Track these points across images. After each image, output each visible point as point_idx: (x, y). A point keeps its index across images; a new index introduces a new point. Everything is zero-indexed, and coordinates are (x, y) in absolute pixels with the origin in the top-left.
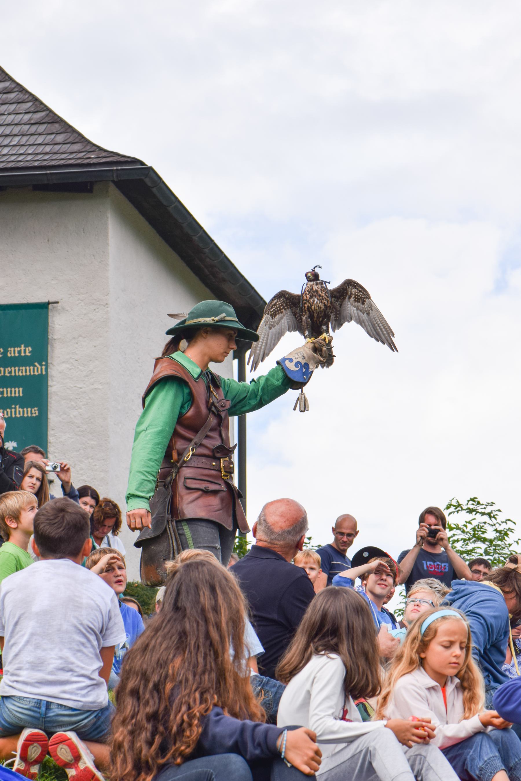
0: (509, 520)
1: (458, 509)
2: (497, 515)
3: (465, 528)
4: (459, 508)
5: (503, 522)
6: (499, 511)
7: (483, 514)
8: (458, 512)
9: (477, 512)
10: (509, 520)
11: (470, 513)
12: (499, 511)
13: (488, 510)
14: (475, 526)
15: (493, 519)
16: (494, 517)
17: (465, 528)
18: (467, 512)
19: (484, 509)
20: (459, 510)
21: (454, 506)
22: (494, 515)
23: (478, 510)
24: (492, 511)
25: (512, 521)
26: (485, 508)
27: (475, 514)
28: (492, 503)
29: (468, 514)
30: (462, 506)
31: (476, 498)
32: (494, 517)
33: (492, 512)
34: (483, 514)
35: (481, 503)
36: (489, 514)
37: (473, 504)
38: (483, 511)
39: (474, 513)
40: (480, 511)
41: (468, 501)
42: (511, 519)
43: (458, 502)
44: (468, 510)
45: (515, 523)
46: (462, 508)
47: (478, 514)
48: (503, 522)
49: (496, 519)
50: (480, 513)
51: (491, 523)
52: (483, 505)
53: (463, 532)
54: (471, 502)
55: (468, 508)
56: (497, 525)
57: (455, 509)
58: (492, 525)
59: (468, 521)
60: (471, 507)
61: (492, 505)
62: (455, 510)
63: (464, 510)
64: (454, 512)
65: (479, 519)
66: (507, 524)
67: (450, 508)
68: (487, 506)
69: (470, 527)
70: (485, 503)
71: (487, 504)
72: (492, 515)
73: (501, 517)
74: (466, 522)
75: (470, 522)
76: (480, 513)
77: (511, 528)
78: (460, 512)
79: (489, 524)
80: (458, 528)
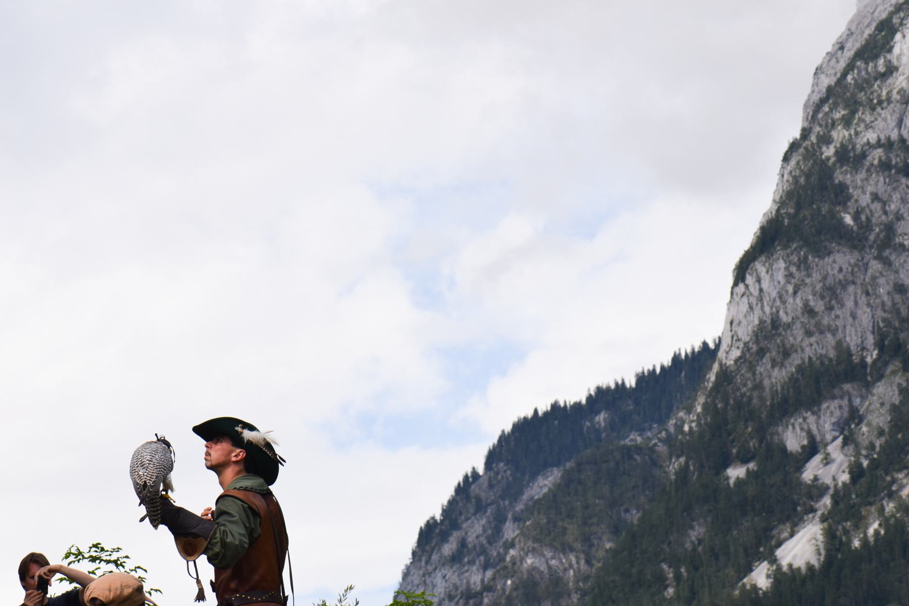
0: (139, 567)
1: (79, 557)
2: (124, 562)
4: (80, 557)
5: (132, 570)
6: (127, 557)
7: (108, 562)
8: (79, 562)
9: (101, 560)
10: (139, 567)
11: (93, 562)
12: (127, 557)
13: (114, 557)
15: (120, 567)
16: (121, 565)
18: (89, 561)
19: (109, 557)
20: (80, 559)
21: (74, 554)
22: (121, 563)
23: (102, 558)
24: (118, 558)
25: (142, 569)
26: (110, 555)
27: (99, 563)
28: (118, 548)
29: (91, 562)
30: (83, 553)
31: (100, 544)
32: (121, 565)
33: (118, 559)
34: (108, 562)
35: (106, 550)
36: (115, 562)
37: (96, 551)
38: (108, 558)
39: (98, 561)
40: (104, 558)
41: (91, 548)
42: (142, 567)
43: (78, 549)
44: (91, 558)
45: (146, 571)
46: (83, 556)
47: (103, 562)
48: (132, 570)
49: (123, 567)
50: (105, 561)
52: (107, 551)
54: (94, 549)
55: (91, 556)
57: (75, 558)
59: (91, 571)
60: (94, 554)
61: (118, 551)
62: (75, 560)
63: (86, 558)
64: (74, 562)
66: (136, 572)
67: (70, 557)
68: (112, 552)
70: (110, 550)
71: (113, 550)
72: (119, 562)
73: (129, 565)
76: (105, 561)
77: (142, 576)
78: (81, 561)
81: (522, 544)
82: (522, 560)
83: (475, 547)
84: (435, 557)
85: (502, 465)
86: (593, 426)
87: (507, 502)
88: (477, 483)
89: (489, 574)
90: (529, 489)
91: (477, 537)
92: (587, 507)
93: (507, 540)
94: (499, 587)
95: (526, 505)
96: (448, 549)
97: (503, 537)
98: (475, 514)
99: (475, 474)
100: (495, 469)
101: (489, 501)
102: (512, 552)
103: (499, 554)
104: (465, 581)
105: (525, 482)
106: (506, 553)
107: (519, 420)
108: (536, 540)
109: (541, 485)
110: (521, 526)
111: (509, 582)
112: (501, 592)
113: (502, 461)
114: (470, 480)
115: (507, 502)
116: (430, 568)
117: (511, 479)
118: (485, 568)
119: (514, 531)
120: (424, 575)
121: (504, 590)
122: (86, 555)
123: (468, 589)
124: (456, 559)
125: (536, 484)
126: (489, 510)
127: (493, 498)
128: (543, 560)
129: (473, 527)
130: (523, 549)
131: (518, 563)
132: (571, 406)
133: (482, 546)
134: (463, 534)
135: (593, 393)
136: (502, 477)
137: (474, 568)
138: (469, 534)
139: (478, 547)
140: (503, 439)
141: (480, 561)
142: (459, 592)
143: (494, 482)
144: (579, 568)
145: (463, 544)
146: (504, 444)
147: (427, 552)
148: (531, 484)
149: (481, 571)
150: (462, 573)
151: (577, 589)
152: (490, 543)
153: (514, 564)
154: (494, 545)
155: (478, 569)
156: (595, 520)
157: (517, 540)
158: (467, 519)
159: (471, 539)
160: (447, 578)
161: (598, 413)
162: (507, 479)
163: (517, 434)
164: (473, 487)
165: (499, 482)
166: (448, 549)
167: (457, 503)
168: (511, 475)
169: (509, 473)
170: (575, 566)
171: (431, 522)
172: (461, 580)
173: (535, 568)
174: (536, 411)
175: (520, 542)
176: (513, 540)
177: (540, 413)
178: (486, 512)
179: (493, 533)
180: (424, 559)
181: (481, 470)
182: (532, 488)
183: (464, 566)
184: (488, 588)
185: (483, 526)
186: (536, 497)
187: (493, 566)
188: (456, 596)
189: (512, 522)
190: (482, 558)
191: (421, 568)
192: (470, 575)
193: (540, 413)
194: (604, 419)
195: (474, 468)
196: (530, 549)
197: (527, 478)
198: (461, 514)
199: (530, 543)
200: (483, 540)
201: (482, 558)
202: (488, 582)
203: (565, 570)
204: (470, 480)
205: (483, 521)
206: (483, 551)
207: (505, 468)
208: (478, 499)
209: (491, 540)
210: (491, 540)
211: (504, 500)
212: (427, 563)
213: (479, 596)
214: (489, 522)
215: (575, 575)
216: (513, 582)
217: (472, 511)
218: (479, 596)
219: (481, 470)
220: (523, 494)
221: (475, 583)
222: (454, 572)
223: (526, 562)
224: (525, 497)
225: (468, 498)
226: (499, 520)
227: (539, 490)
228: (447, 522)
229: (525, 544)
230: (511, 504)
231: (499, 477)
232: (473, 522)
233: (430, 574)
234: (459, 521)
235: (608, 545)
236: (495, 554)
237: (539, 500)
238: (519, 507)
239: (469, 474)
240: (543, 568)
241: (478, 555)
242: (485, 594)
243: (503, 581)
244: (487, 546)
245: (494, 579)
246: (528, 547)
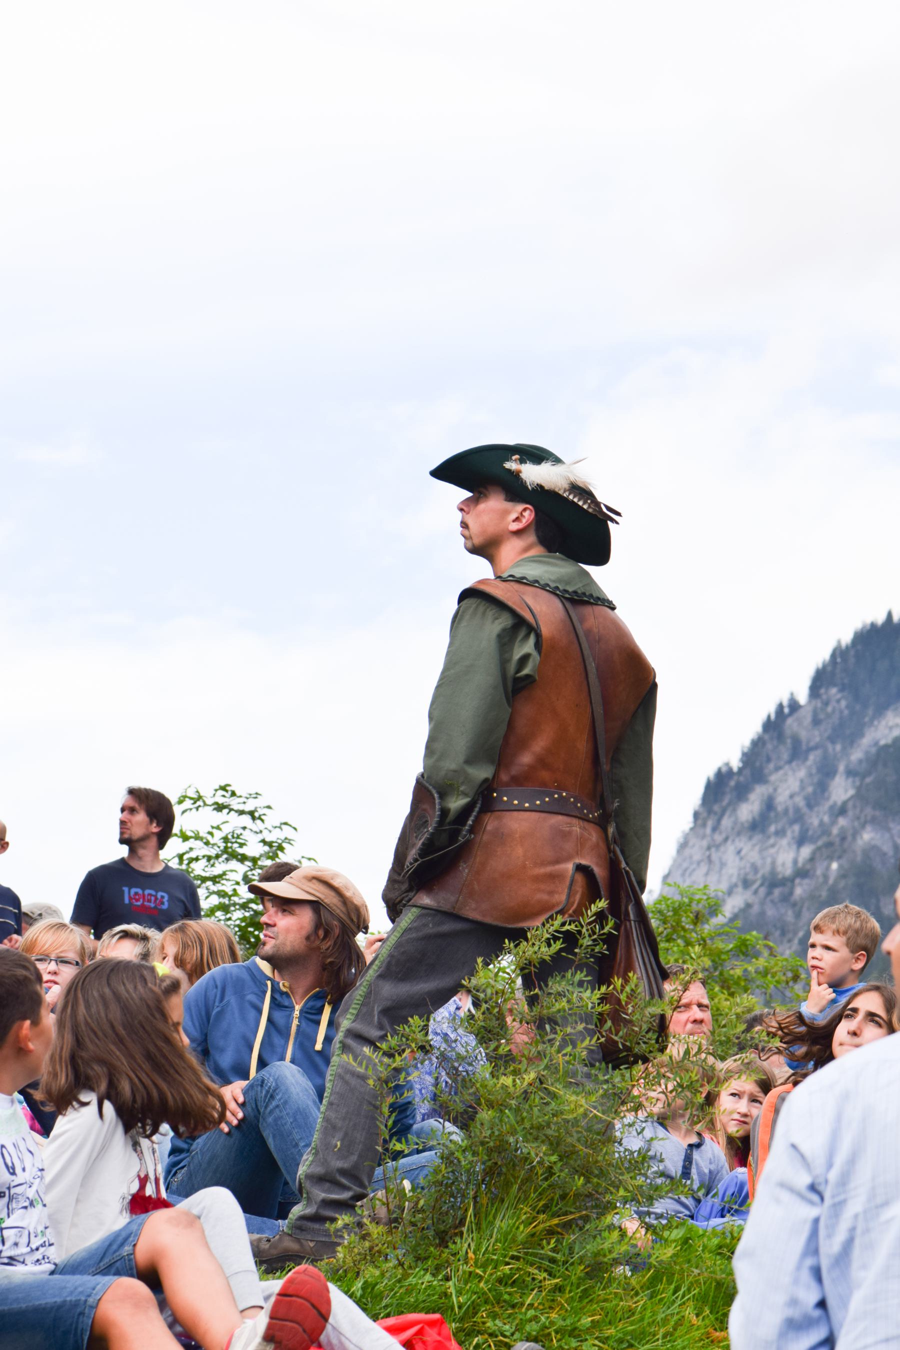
0: (286, 824)
1: (198, 803)
2: (264, 815)
3: (209, 838)
4: (200, 803)
5: (276, 827)
6: (269, 807)
7: (241, 813)
8: (197, 808)
9: (231, 810)
10: (286, 824)
11: (218, 811)
12: (269, 807)
13: (248, 807)
14: (227, 835)
15: (258, 822)
16: (259, 818)
17: (209, 838)
18: (214, 809)
19: (243, 805)
20: (200, 806)
21: (191, 798)
22: (260, 816)
23: (231, 807)
24: (256, 808)
25: (290, 826)
26: (244, 803)
28: (257, 794)
29: (215, 812)
30: (204, 798)
31: (229, 785)
32: (259, 818)
33: (256, 810)
34: (241, 813)
35: (238, 794)
36: (251, 814)
37: (224, 796)
38: (241, 807)
39: (226, 811)
40: (236, 807)
41: (216, 790)
42: (290, 823)
43: (197, 792)
44: (216, 806)
45: (295, 829)
46: (204, 802)
47: (232, 812)
48: (276, 827)
49: (263, 821)
50: (236, 811)
51: (255, 829)
52: (240, 796)
53: (207, 843)
54: (222, 792)
55: (216, 803)
56: (265, 832)
57: (193, 804)
58: (256, 832)
59: (215, 825)
60: (221, 800)
61: (256, 798)
62: (192, 806)
63: (208, 805)
64: (191, 809)
65: (233, 822)
66: (282, 830)
67: (184, 803)
69: (218, 835)
70: (244, 795)
71: (248, 796)
72: (257, 815)
73: (272, 819)
74: (213, 827)
75: (218, 828)
76: (236, 811)
77: (289, 837)
78: (200, 809)
79: (251, 830)
80: (197, 837)
81: (858, 810)
82: (855, 834)
83: (786, 811)
84: (726, 822)
85: (834, 691)
87: (838, 747)
88: (796, 715)
89: (806, 851)
90: (873, 729)
91: (792, 796)
93: (835, 803)
94: (819, 872)
95: (867, 753)
96: (748, 810)
97: (828, 799)
98: (790, 762)
99: (794, 706)
100: (824, 697)
101: (812, 744)
102: (842, 822)
103: (821, 823)
104: (769, 860)
105: (867, 719)
106: (834, 822)
108: (877, 805)
109: (891, 723)
110: (858, 783)
111: (835, 866)
112: (821, 880)
113: (835, 685)
114: (786, 710)
115: (838, 747)
116: (718, 838)
117: (846, 712)
118: (801, 842)
119: (846, 791)
120: (709, 848)
121: (826, 877)
122: (209, 801)
123: (773, 872)
124: (757, 826)
125: (883, 723)
126: (811, 757)
127: (817, 739)
128: (887, 836)
129: (786, 780)
130: (858, 818)
131: (850, 838)
133: (797, 810)
134: (771, 790)
136: (834, 711)
137: (784, 842)
138: (780, 790)
139: (791, 811)
140: (838, 653)
141: (793, 832)
142: (759, 875)
143: (822, 716)
145: (769, 805)
146: (839, 660)
147: (715, 813)
148: (876, 723)
149: (794, 847)
150: (766, 848)
152: (810, 806)
153: (843, 839)
154: (816, 809)
155: (789, 844)
157: (850, 804)
158: (778, 768)
159: (782, 799)
160: (743, 853)
162: (841, 712)
163: (859, 647)
164: (789, 721)
165: (828, 716)
166: (748, 810)
167: (764, 743)
168: (847, 707)
169: (843, 703)
171: (724, 770)
172: (763, 858)
173: (874, 848)
175: (855, 807)
176: (845, 803)
178: (806, 759)
179: (815, 793)
180: (710, 824)
181: (803, 698)
183: (769, 837)
184: (802, 873)
185: (802, 781)
186: (882, 742)
187: (813, 840)
188: (754, 882)
189: (844, 777)
190: (797, 828)
191: (704, 837)
192: (777, 852)
195: (792, 694)
196: (869, 818)
197: (870, 712)
198: (769, 760)
199: (869, 811)
200: (800, 801)
201: (797, 828)
202: (804, 865)
204: (786, 710)
205: (802, 773)
206: (799, 818)
207: (839, 696)
208: (796, 741)
209: (811, 803)
210: (811, 803)
211: (833, 742)
212: (715, 829)
213: (789, 884)
214: (810, 775)
216: (840, 867)
217: (785, 756)
218: (789, 884)
219: (803, 698)
220: (862, 735)
221: (783, 864)
222: (754, 845)
223: (862, 838)
224: (866, 741)
225: (780, 737)
226: (826, 772)
227: (887, 731)
228: (747, 772)
229: (861, 811)
230: (844, 749)
231: (829, 709)
232: (786, 774)
233: (718, 847)
234: (766, 771)
236: (816, 822)
237: (886, 746)
238: (857, 755)
239: (785, 703)
240: (887, 848)
241: (792, 822)
242: (797, 881)
243: (825, 863)
244: (805, 810)
245: (812, 859)
246: (866, 816)
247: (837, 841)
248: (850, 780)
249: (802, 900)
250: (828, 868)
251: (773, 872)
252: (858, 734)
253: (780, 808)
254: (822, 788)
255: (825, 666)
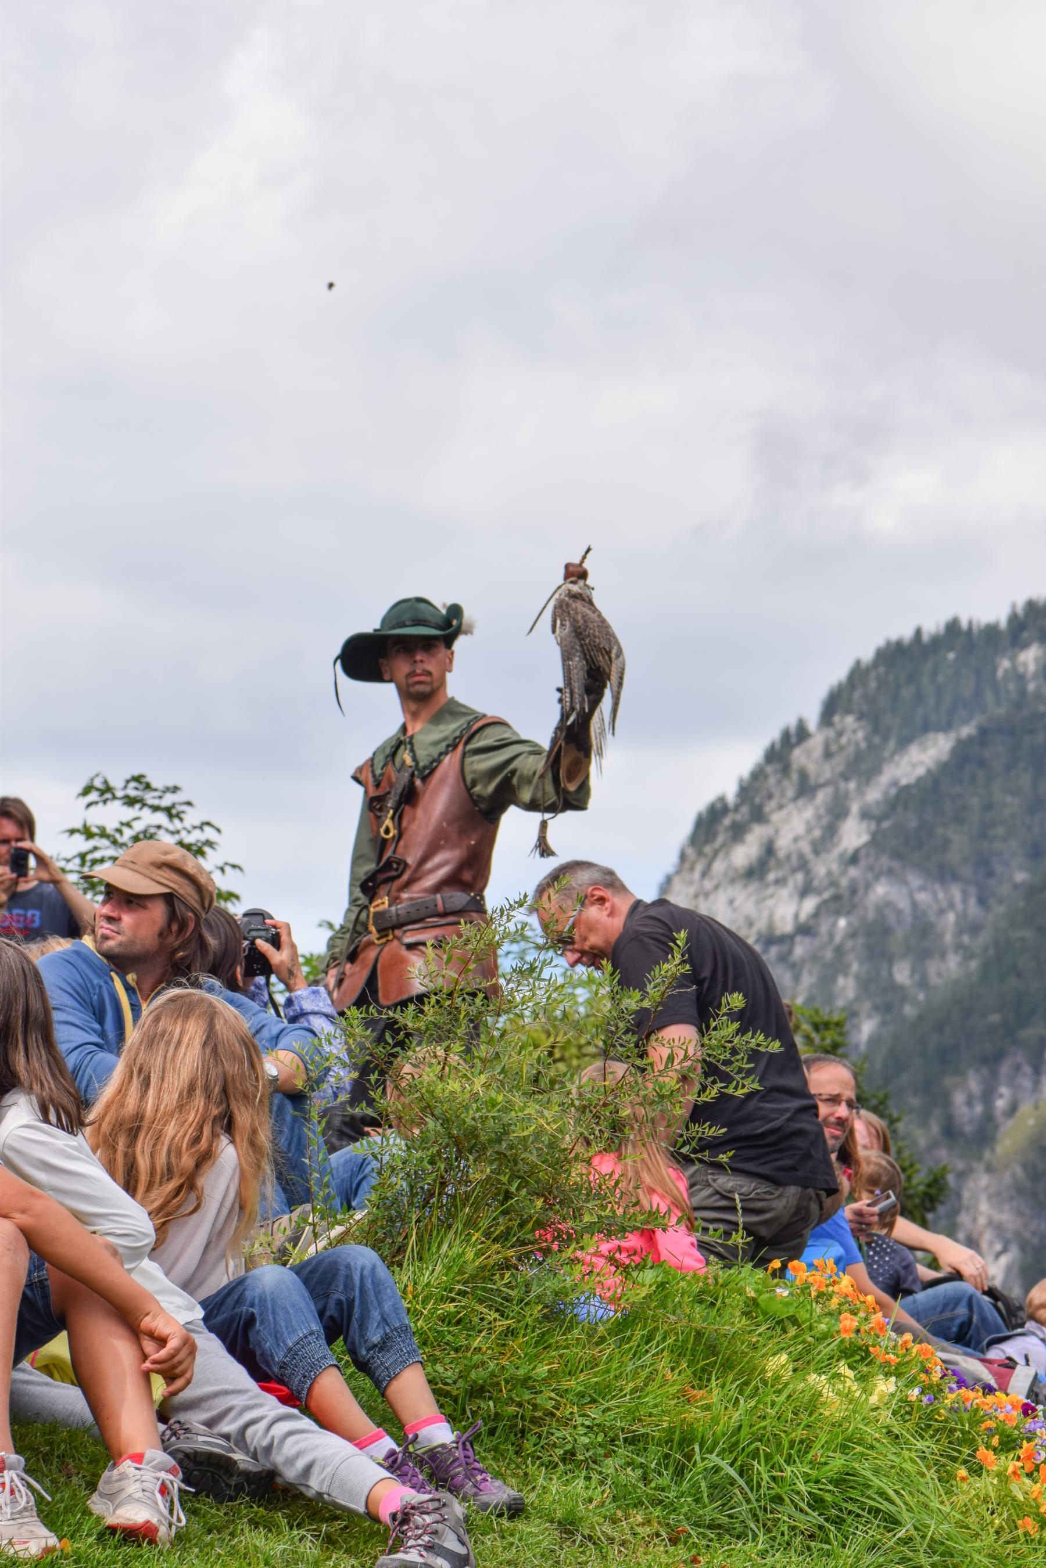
0: (208, 824)
2: (183, 812)
3: (117, 836)
4: (108, 796)
6: (189, 804)
7: (156, 809)
8: (105, 802)
9: (144, 805)
10: (208, 824)
12: (189, 804)
13: (167, 800)
14: (138, 833)
17: (117, 836)
18: (125, 804)
21: (98, 789)
26: (160, 797)
27: (141, 809)
33: (173, 806)
37: (136, 788)
38: (156, 802)
39: (138, 806)
40: (150, 802)
41: (128, 782)
45: (219, 830)
48: (195, 827)
49: (181, 820)
51: (171, 827)
52: (156, 790)
53: (115, 842)
54: (133, 784)
55: (127, 797)
56: (183, 833)
58: (173, 833)
59: (125, 820)
60: (133, 793)
65: (148, 818)
68: (164, 792)
69: (128, 833)
72: (174, 812)
73: (192, 817)
74: (122, 824)
75: (128, 825)
78: (109, 803)
79: (167, 830)
80: (103, 834)
82: (868, 886)
83: (788, 857)
84: (719, 866)
86: (1014, 667)
87: (852, 785)
91: (796, 840)
92: (988, 807)
93: (845, 851)
95: (886, 793)
96: (744, 854)
98: (795, 799)
101: (821, 780)
102: (853, 872)
103: (830, 873)
104: (765, 914)
106: (844, 873)
107: (889, 643)
108: (896, 855)
111: (842, 923)
112: (825, 938)
114: (794, 740)
116: (708, 885)
117: (863, 745)
118: (805, 892)
119: (859, 836)
120: (696, 896)
121: (831, 935)
122: (120, 794)
123: (771, 926)
124: (755, 873)
128: (904, 890)
131: (861, 892)
132: (981, 631)
133: (801, 856)
135: (1020, 610)
136: (849, 741)
137: (784, 893)
138: (782, 832)
143: (834, 748)
144: (965, 911)
145: (769, 849)
147: (705, 855)
148: (897, 758)
149: (796, 898)
150: (763, 900)
151: (959, 947)
152: (816, 852)
153: (853, 891)
155: (791, 896)
156: (1000, 830)
157: (863, 853)
158: (781, 807)
159: (784, 844)
160: (737, 903)
161: (1025, 646)
163: (882, 670)
165: (841, 749)
166: (744, 854)
167: (766, 777)
169: (860, 735)
170: (959, 906)
171: (719, 806)
173: (888, 904)
174: (918, 632)
175: (868, 855)
177: (925, 638)
180: (699, 868)
182: (898, 764)
183: (767, 886)
184: (805, 930)
185: (808, 822)
186: (904, 782)
187: (818, 892)
190: (800, 877)
191: (691, 883)
193: (925, 638)
194: (1036, 660)
197: (891, 744)
198: (770, 796)
199: (885, 861)
200: (806, 847)
201: (800, 877)
203: (941, 912)
205: (809, 813)
208: (803, 776)
209: (819, 848)
210: (819, 848)
212: (704, 874)
214: (819, 817)
215: (957, 923)
216: (849, 924)
217: (790, 793)
225: (786, 770)
226: (837, 812)
228: (745, 810)
231: (844, 740)
232: (789, 814)
233: (707, 895)
235: (1020, 877)
237: (908, 787)
238: (874, 795)
239: (793, 730)
240: (904, 904)
241: (794, 871)
242: (798, 939)
245: (816, 914)
247: (846, 894)
248: (864, 824)
249: (803, 961)
250: (834, 924)
251: (771, 926)
252: (876, 770)
253: (781, 854)
254: (831, 832)
255: (840, 685)
